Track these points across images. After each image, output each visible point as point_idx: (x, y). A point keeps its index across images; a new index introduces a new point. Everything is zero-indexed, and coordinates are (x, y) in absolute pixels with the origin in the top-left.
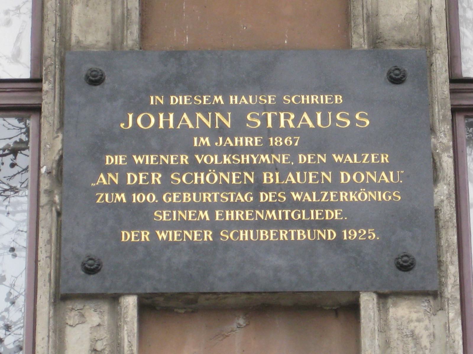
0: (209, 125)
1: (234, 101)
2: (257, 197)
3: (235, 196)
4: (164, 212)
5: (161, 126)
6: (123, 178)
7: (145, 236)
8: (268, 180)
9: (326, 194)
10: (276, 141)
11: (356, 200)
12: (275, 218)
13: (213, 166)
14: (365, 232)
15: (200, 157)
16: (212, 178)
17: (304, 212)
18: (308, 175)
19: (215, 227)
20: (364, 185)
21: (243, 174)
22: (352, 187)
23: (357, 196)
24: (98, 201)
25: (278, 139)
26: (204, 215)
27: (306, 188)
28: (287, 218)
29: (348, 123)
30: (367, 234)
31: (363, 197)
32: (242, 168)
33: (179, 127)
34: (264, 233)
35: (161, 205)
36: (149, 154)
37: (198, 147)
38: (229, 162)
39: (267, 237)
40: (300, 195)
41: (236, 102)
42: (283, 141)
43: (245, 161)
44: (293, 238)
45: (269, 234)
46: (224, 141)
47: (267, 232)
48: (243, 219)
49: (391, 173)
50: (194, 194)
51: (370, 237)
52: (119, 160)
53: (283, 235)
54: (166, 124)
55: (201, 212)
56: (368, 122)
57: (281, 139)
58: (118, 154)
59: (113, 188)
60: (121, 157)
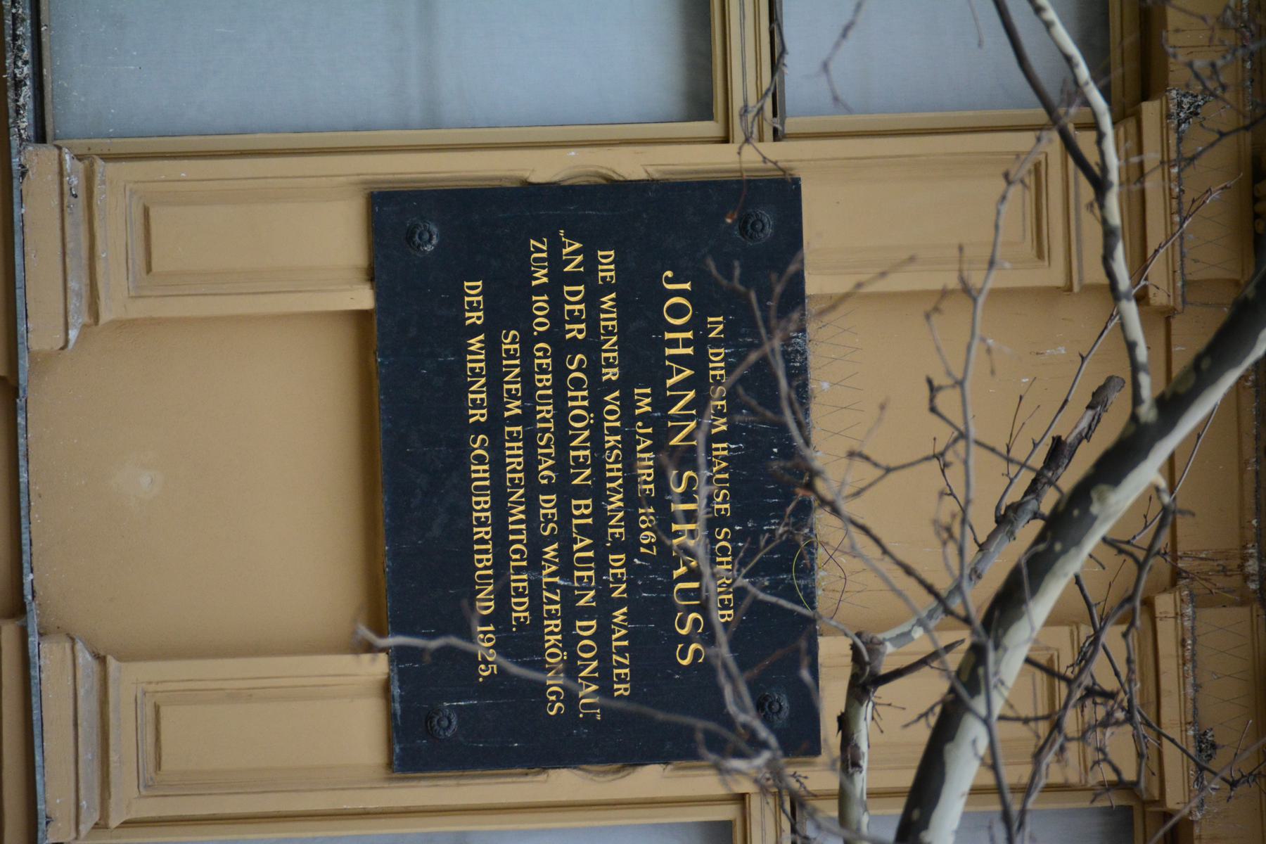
0: (673, 411)
1: (717, 449)
2: (547, 490)
3: (548, 455)
4: (517, 346)
5: (668, 336)
6: (574, 279)
7: (475, 318)
8: (578, 507)
9: (557, 598)
10: (647, 515)
11: (547, 645)
12: (511, 519)
13: (600, 420)
16: (578, 418)
17: (525, 563)
18: (589, 569)
19: (494, 427)
20: (573, 657)
22: (570, 640)
24: (532, 242)
26: (514, 408)
27: (566, 569)
28: (511, 537)
29: (684, 632)
34: (486, 502)
35: (528, 342)
36: (619, 319)
38: (607, 446)
40: (554, 557)
41: (715, 453)
42: (648, 529)
43: (611, 470)
44: (476, 547)
45: (483, 510)
46: (646, 436)
47: (486, 506)
48: (508, 468)
50: (550, 392)
51: (483, 666)
52: (607, 270)
53: (482, 532)
54: (674, 343)
55: (518, 403)
56: (685, 663)
58: (616, 270)
59: (555, 261)
60: (613, 273)
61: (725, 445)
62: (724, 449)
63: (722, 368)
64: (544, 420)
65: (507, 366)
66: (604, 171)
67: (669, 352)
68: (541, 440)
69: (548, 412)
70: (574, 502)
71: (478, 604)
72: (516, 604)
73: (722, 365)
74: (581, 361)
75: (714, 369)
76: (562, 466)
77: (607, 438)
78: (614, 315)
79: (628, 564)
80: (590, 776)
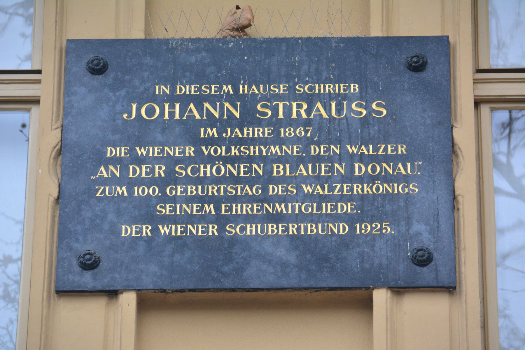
0: (217, 115)
1: (244, 91)
2: (265, 190)
3: (242, 189)
4: (168, 206)
5: (167, 117)
7: (146, 230)
11: (370, 192)
12: (284, 212)
14: (379, 226)
16: (218, 171)
17: (315, 205)
18: (320, 167)
23: (371, 188)
24: (98, 195)
25: (290, 130)
28: (297, 212)
30: (381, 229)
31: (378, 189)
32: (250, 160)
33: (185, 118)
34: (272, 227)
35: (164, 199)
37: (204, 138)
38: (238, 154)
41: (246, 92)
42: (295, 132)
43: (254, 152)
44: (303, 233)
45: (278, 228)
46: (232, 132)
47: (275, 226)
48: (250, 213)
49: (409, 165)
50: (200, 187)
51: (384, 231)
52: (121, 152)
53: (292, 229)
54: (172, 114)
55: (206, 206)
56: (385, 112)
57: (292, 130)
58: (120, 146)
59: (113, 181)
61: (241, 86)
62: (244, 87)
63: (190, 87)
64: (218, 190)
65: (181, 212)
66: (54, 154)
67: (177, 117)
68: (232, 193)
69: (213, 188)
70: (275, 174)
71: (341, 232)
72: (342, 210)
73: (188, 87)
74: (180, 168)
75: (190, 91)
76: (251, 182)
77: (233, 154)
78: (151, 149)
79: (318, 144)
80: (460, 171)
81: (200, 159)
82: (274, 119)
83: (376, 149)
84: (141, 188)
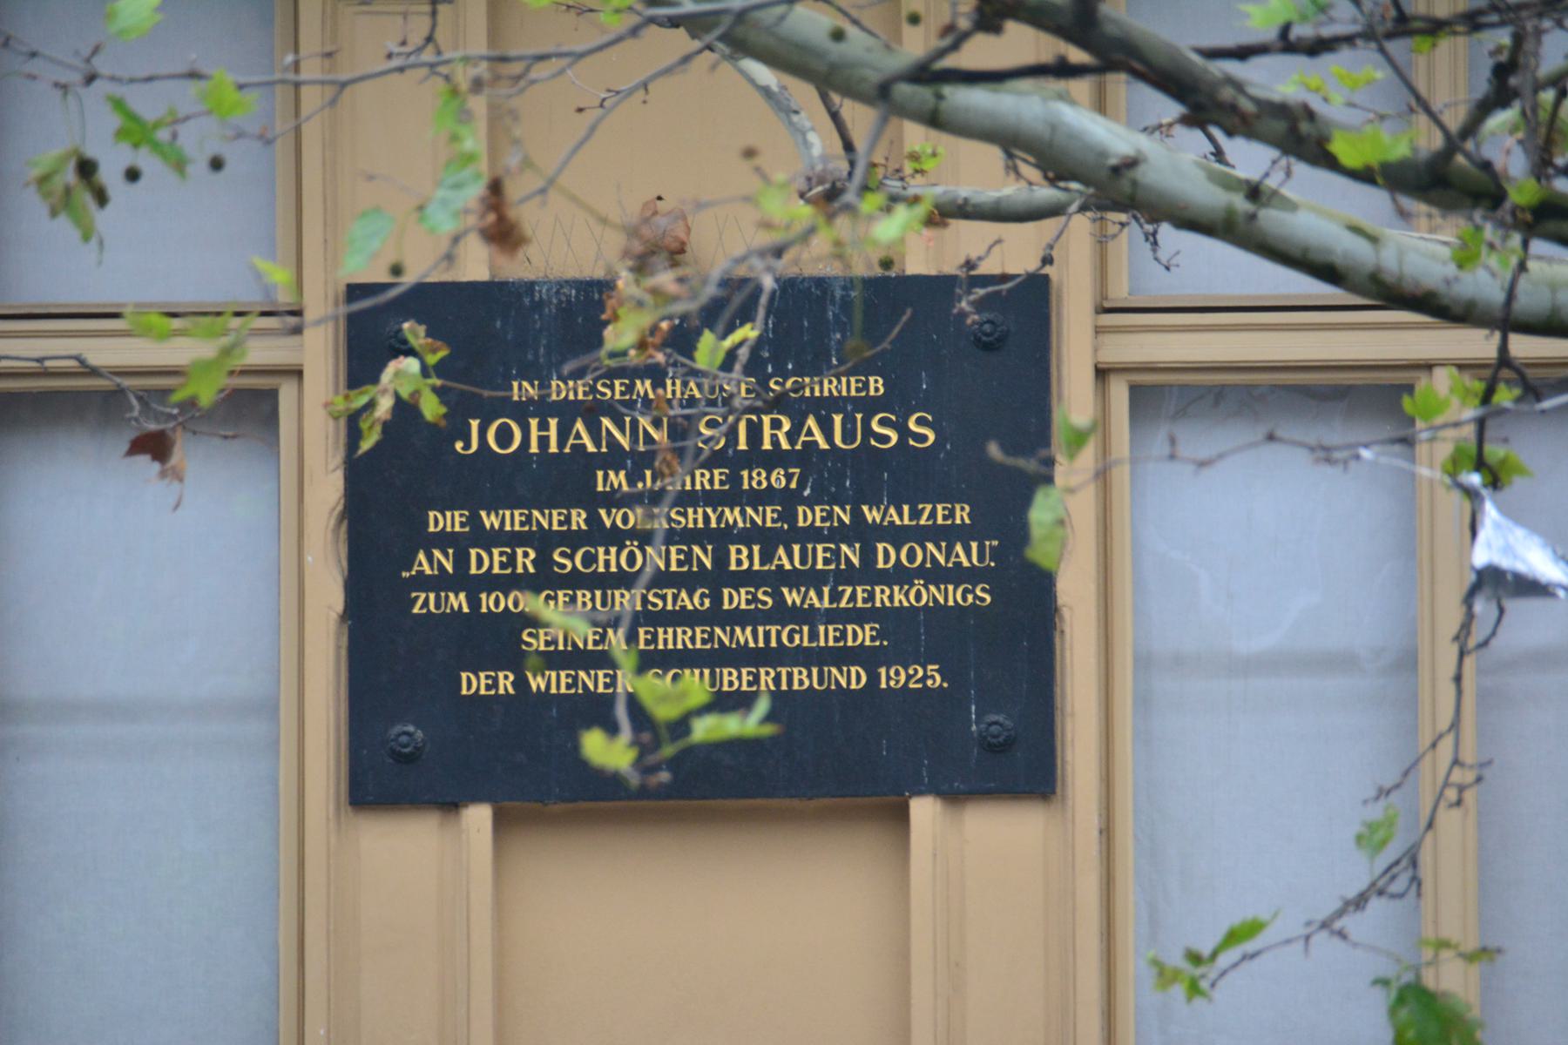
2: (717, 599)
3: (675, 597)
5: (534, 449)
6: (462, 561)
7: (506, 682)
9: (849, 590)
10: (754, 479)
12: (752, 645)
13: (633, 534)
14: (921, 673)
15: (609, 514)
20: (921, 572)
21: (691, 550)
22: (900, 576)
23: (907, 595)
24: (416, 610)
25: (759, 474)
27: (812, 579)
28: (774, 644)
30: (925, 677)
31: (918, 596)
33: (567, 450)
36: (512, 507)
37: (604, 492)
39: (736, 684)
40: (799, 592)
42: (768, 478)
43: (695, 521)
44: (784, 687)
45: (739, 678)
49: (974, 545)
50: (598, 593)
51: (929, 682)
52: (451, 521)
54: (543, 442)
56: (932, 437)
57: (764, 475)
58: (452, 509)
59: (441, 583)
60: (457, 513)
61: (669, 382)
62: (674, 384)
65: (565, 645)
66: (333, 522)
67: (553, 449)
70: (733, 567)
71: (853, 686)
74: (563, 554)
76: (686, 581)
78: (508, 513)
81: (597, 534)
82: (730, 452)
83: (916, 514)
84: (493, 597)
